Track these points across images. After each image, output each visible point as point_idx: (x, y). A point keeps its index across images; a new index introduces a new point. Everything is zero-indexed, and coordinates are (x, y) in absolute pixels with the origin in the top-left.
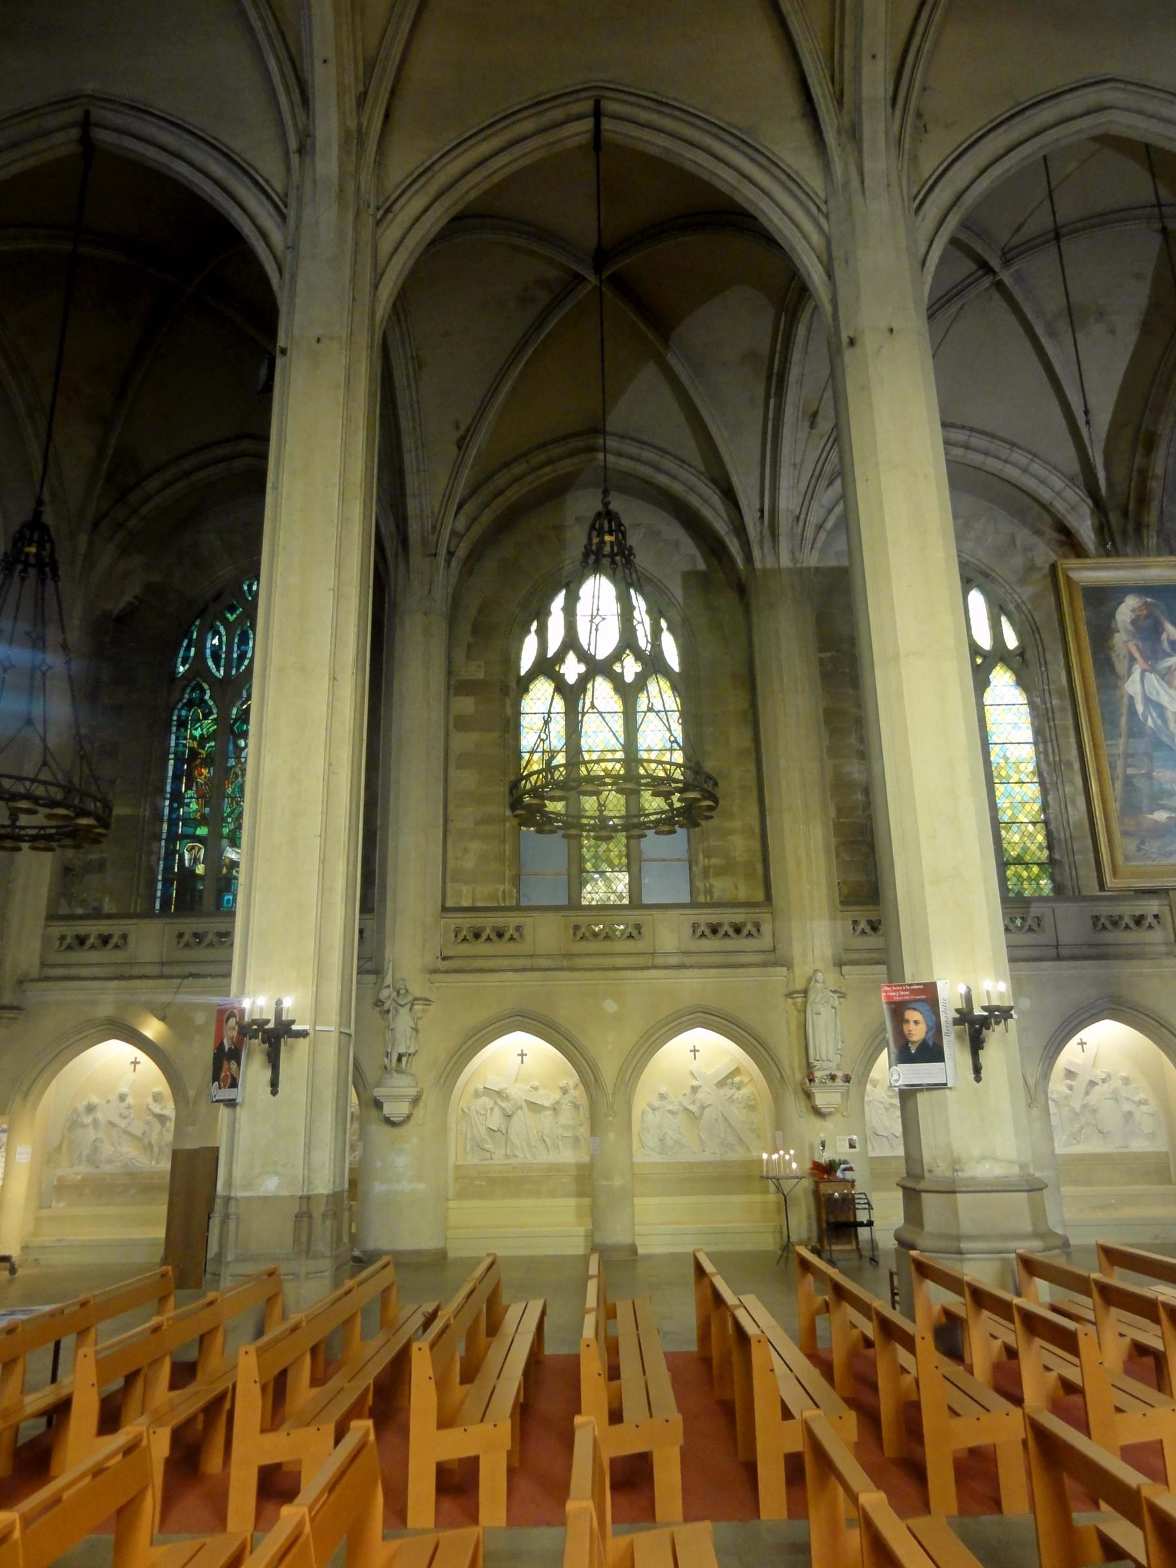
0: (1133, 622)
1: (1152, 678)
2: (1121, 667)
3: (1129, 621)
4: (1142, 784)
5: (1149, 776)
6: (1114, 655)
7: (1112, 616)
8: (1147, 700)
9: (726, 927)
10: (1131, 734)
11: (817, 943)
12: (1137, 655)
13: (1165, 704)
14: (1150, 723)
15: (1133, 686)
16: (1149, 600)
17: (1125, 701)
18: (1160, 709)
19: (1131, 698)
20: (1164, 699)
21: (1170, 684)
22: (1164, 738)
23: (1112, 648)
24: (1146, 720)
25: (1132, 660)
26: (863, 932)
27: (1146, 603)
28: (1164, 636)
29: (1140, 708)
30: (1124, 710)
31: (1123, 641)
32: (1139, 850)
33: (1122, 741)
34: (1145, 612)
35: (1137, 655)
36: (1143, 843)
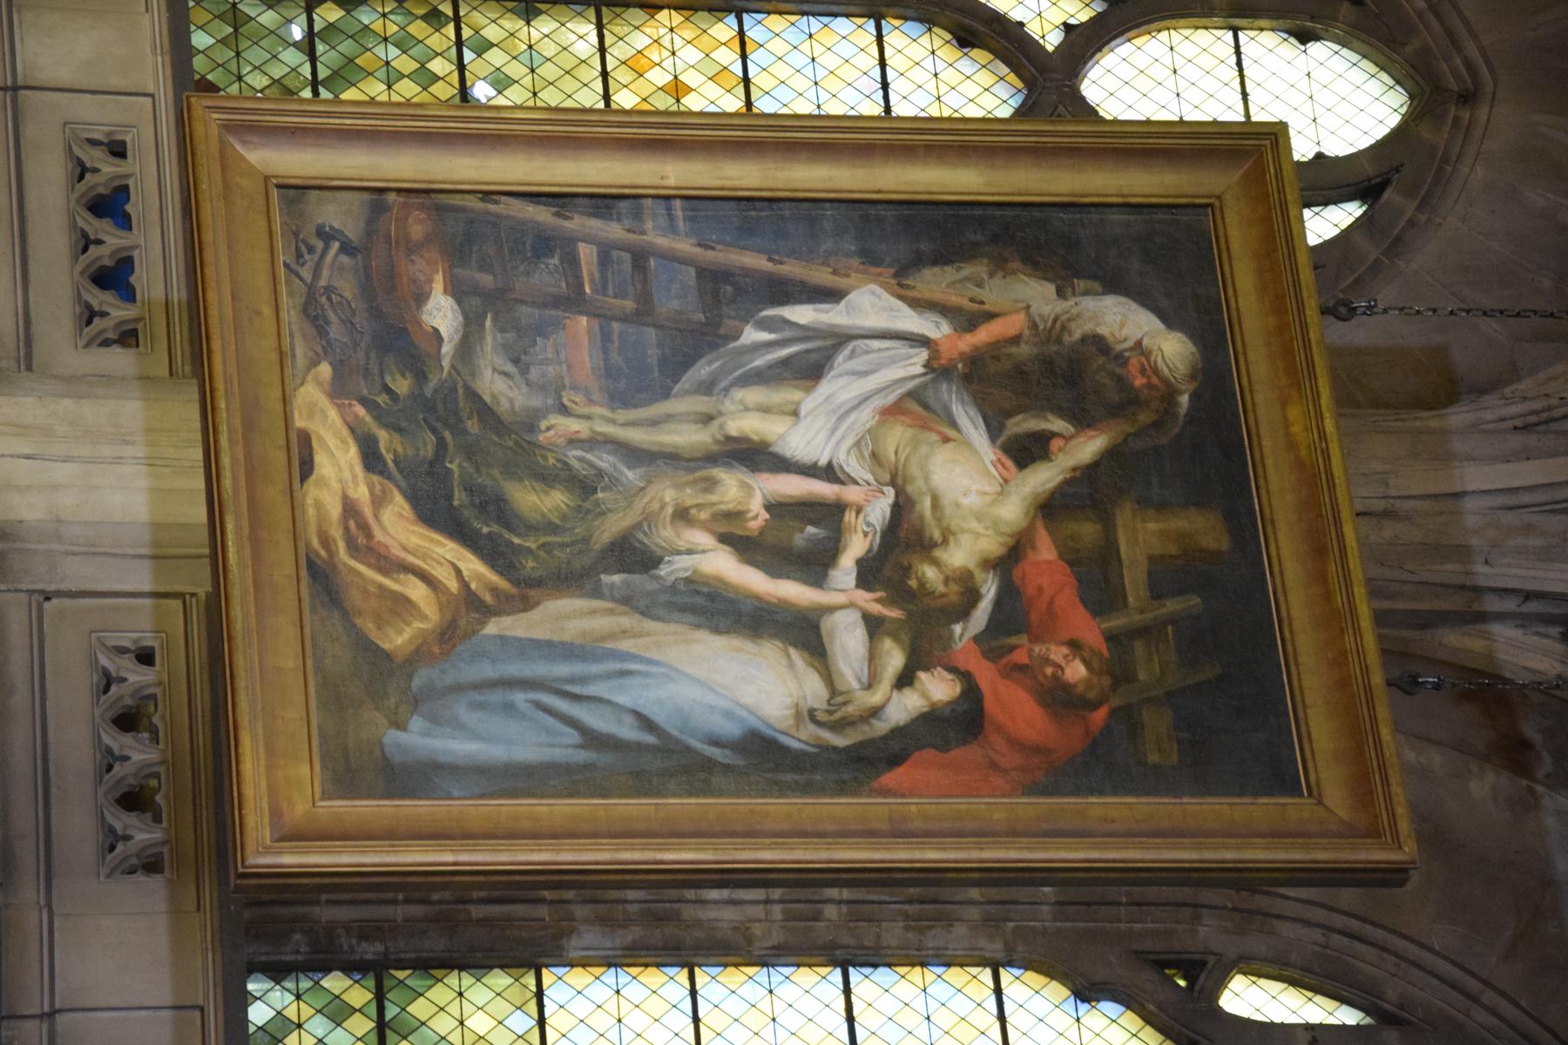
0: (1098, 343)
1: (914, 364)
2: (935, 281)
3: (1103, 330)
4: (546, 277)
5: (574, 301)
6: (979, 269)
7: (1113, 284)
8: (840, 339)
9: (112, 239)
10: (713, 280)
11: (62, 472)
12: (984, 335)
13: (825, 388)
14: (752, 335)
15: (870, 305)
16: (1184, 400)
17: (821, 276)
18: (809, 369)
19: (832, 295)
20: (838, 387)
21: (892, 412)
22: (703, 369)
23: (999, 265)
24: (764, 325)
25: (968, 320)
26: (108, 681)
27: (1169, 394)
28: (1057, 424)
29: (802, 314)
30: (791, 269)
31: (1025, 301)
32: (326, 235)
33: (684, 246)
34: (1139, 382)
35: (984, 335)
36: (347, 249)
